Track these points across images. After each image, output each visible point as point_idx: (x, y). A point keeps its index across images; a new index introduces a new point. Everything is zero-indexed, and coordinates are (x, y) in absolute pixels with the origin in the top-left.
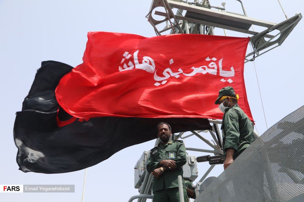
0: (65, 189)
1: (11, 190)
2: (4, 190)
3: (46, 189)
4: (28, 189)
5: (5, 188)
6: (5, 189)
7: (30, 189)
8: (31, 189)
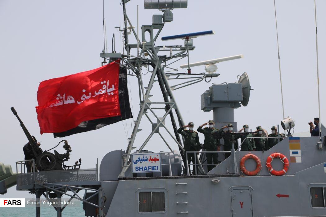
1: (11, 205)
2: (5, 204)
5: (6, 202)
6: (5, 203)
7: (32, 203)
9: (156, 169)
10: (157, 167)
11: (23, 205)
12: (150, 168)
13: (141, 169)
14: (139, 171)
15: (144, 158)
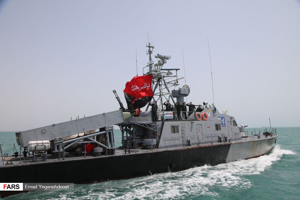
1: (10, 189)
2: (4, 188)
5: (5, 186)
6: (5, 187)
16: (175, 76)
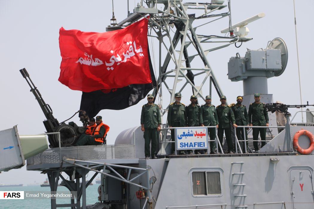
0: (67, 196)
1: (11, 197)
2: (4, 197)
3: (48, 196)
4: (29, 196)
5: (5, 194)
7: (31, 195)
8: (32, 195)
9: (203, 145)
10: (204, 143)
11: (22, 197)
12: (196, 144)
13: (186, 145)
14: (184, 148)
15: (189, 132)
16: (224, 15)
